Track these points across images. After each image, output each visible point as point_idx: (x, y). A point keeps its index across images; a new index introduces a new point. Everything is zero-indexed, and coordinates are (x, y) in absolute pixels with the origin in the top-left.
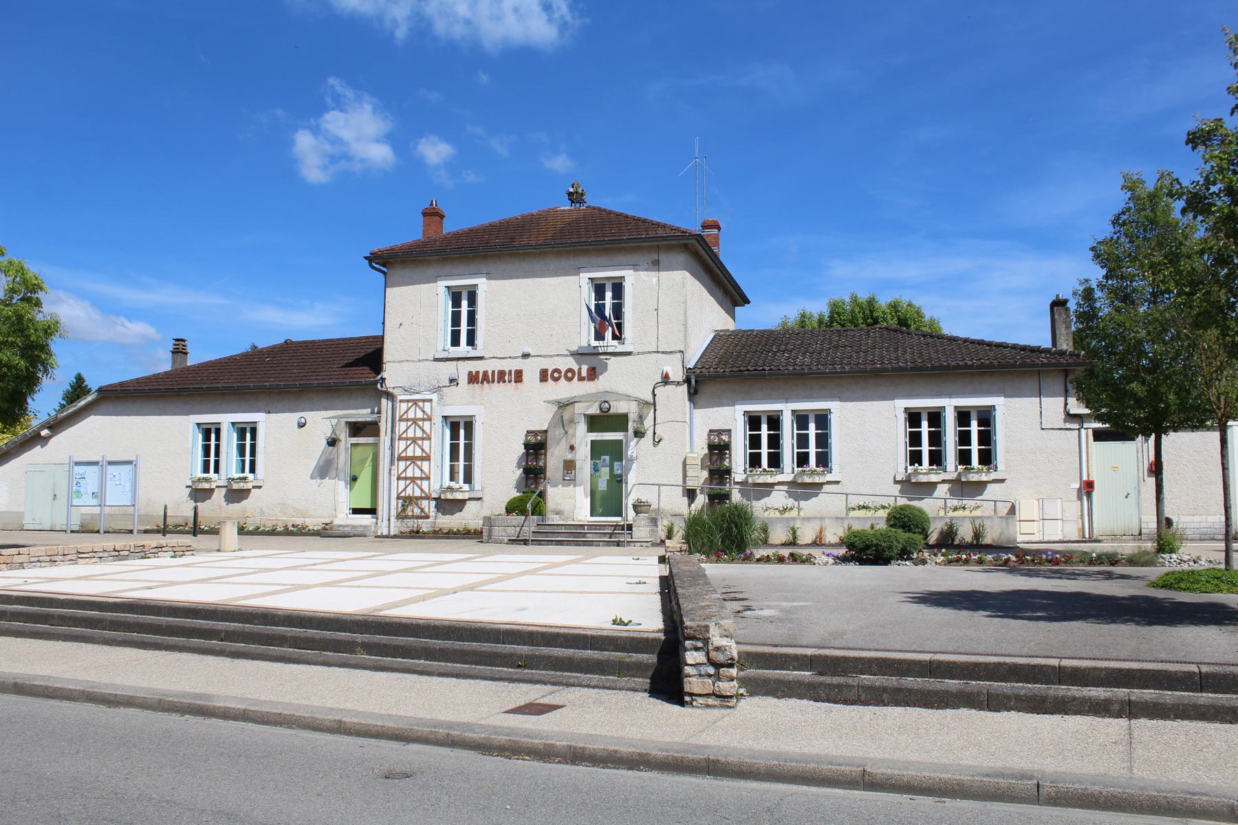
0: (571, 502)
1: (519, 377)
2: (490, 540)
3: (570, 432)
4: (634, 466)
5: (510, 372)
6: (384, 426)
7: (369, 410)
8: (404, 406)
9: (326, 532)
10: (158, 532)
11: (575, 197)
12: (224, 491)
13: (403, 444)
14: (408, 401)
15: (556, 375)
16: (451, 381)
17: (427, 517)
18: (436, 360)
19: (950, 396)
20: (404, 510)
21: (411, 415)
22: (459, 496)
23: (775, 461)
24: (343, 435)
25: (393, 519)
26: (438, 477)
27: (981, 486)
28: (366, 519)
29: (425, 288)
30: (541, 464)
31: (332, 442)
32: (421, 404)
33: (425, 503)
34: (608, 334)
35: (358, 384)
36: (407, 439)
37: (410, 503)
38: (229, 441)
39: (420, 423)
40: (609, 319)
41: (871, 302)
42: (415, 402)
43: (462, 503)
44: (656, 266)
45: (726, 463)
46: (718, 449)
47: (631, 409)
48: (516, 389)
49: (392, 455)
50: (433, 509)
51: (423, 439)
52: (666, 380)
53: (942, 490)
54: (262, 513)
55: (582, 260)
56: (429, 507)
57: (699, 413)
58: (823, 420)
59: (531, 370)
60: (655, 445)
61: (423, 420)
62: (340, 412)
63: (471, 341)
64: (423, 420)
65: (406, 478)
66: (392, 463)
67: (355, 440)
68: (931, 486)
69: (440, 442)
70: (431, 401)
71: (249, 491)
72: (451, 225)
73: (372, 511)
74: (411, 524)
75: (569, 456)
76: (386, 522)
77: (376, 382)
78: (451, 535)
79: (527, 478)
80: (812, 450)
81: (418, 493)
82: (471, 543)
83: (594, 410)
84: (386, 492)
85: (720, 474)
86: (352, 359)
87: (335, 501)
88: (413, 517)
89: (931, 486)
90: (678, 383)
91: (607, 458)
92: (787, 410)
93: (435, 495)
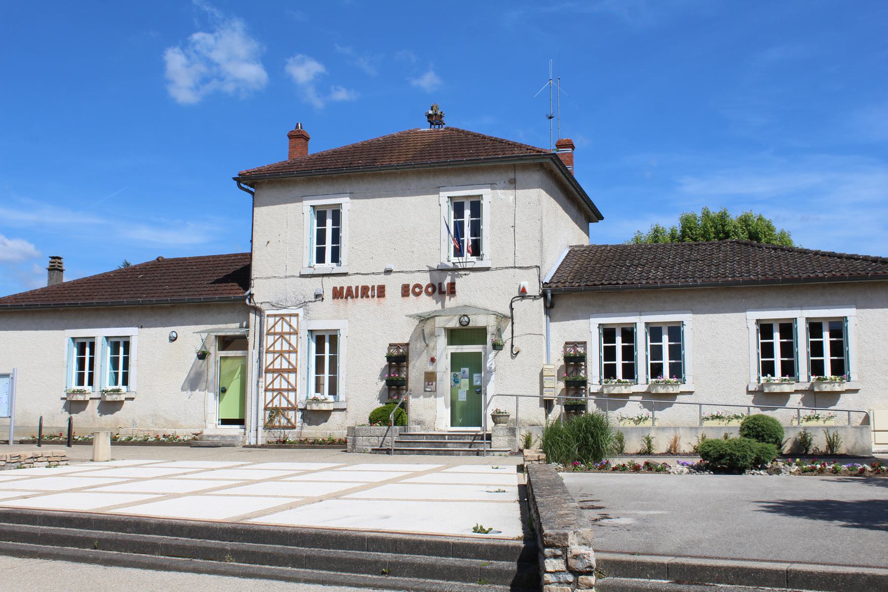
0: (432, 412)
1: (381, 292)
2: (354, 449)
3: (431, 345)
5: (373, 287)
6: (252, 340)
7: (238, 325)
8: (271, 321)
9: (196, 442)
10: (33, 442)
11: (435, 119)
12: (97, 402)
13: (270, 358)
14: (275, 316)
15: (417, 290)
16: (317, 296)
17: (294, 427)
18: (302, 276)
19: (801, 307)
20: (271, 421)
21: (278, 329)
22: (324, 407)
23: (630, 372)
25: (260, 429)
26: (304, 388)
27: (834, 396)
28: (235, 430)
30: (403, 376)
31: (202, 356)
32: (288, 319)
33: (291, 414)
35: (227, 299)
36: (274, 352)
37: (277, 414)
38: (103, 355)
39: (287, 337)
41: (723, 217)
42: (282, 317)
43: (328, 413)
44: (513, 184)
46: (574, 361)
49: (260, 367)
50: (299, 419)
51: (289, 352)
52: (523, 294)
53: (795, 400)
54: (134, 423)
55: (441, 180)
56: (296, 417)
57: (555, 326)
58: (676, 332)
59: (393, 285)
60: (512, 357)
61: (290, 334)
62: (210, 327)
63: (336, 258)
64: (290, 334)
65: (273, 390)
66: (260, 375)
67: (224, 353)
68: (785, 396)
69: (305, 355)
70: (297, 315)
71: (121, 402)
72: (315, 148)
73: (241, 422)
74: (278, 434)
75: (430, 368)
76: (253, 433)
77: (244, 298)
79: (390, 390)
80: (666, 361)
81: (284, 404)
83: (454, 324)
84: (254, 403)
85: (575, 385)
86: (222, 276)
87: (205, 412)
88: (280, 427)
89: (785, 396)
90: (535, 298)
91: (467, 370)
92: (640, 322)
93: (303, 407)
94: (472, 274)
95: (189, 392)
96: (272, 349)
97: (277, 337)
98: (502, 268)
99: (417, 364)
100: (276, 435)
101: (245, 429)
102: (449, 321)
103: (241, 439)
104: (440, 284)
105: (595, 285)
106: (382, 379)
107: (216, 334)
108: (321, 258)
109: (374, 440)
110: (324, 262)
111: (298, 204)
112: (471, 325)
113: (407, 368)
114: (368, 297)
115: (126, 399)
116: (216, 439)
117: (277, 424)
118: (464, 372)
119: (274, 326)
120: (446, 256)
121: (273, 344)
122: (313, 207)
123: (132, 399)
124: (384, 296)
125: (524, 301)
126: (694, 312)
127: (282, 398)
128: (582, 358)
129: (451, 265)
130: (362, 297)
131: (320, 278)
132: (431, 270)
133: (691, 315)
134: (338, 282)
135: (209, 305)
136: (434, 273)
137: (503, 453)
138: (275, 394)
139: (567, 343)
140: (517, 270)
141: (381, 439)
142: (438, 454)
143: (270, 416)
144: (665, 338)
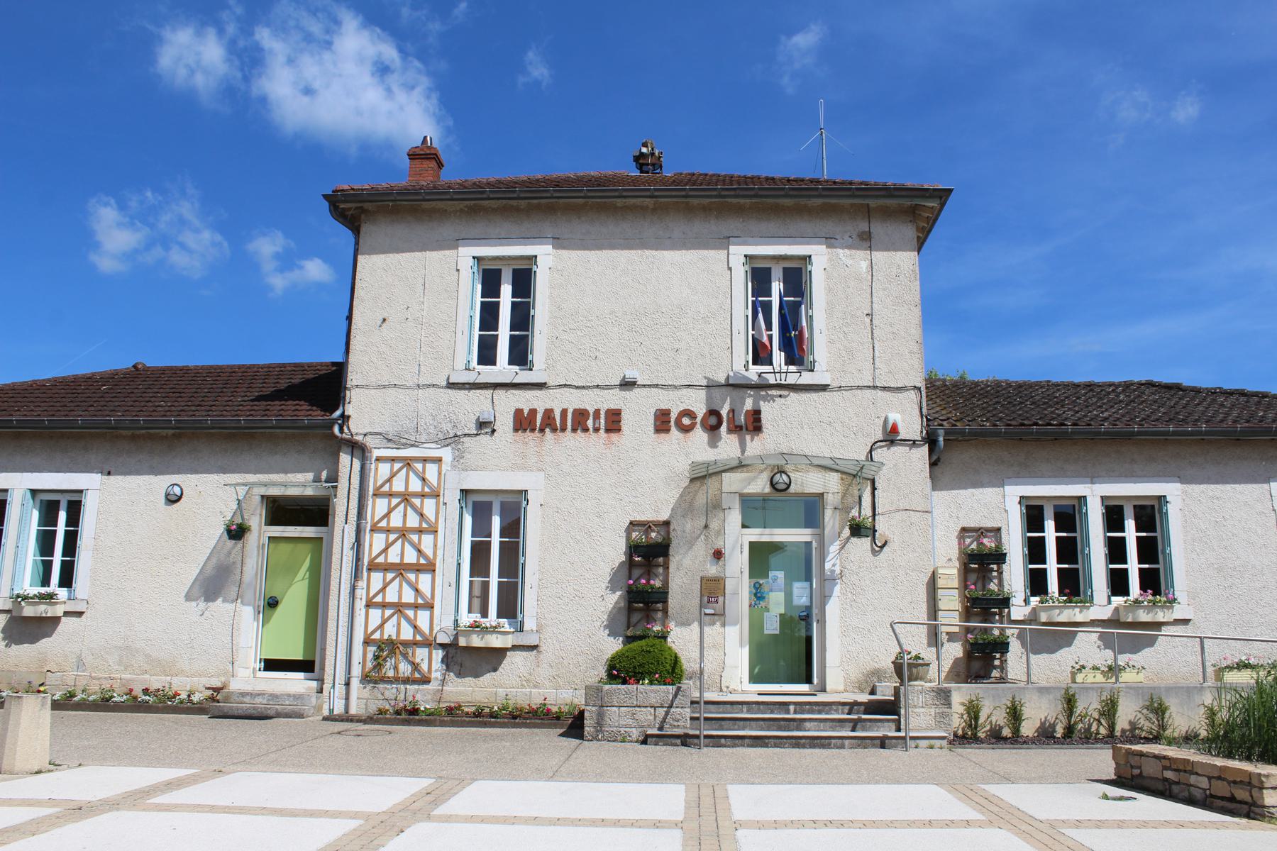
0: (721, 657)
1: (614, 421)
3: (714, 525)
4: (837, 589)
5: (597, 412)
6: (343, 508)
7: (310, 476)
8: (384, 469)
9: (216, 706)
13: (379, 541)
14: (393, 460)
15: (686, 421)
16: (482, 425)
17: (426, 681)
18: (452, 386)
21: (398, 486)
22: (495, 641)
23: (1072, 585)
24: (256, 519)
25: (355, 683)
26: (449, 606)
28: (295, 682)
29: (435, 259)
30: (657, 583)
31: (237, 532)
32: (419, 466)
33: (421, 654)
34: (778, 357)
36: (388, 531)
37: (392, 653)
39: (417, 501)
40: (785, 326)
42: (408, 462)
44: (866, 240)
45: (993, 586)
46: (981, 560)
47: (830, 485)
48: (609, 444)
49: (358, 559)
50: (437, 663)
51: (420, 531)
52: (891, 436)
54: (80, 663)
55: (732, 225)
58: (1150, 515)
59: (638, 411)
60: (874, 553)
61: (423, 496)
62: (251, 478)
63: (520, 354)
64: (423, 496)
65: (384, 605)
66: (357, 575)
67: (277, 531)
69: (451, 540)
70: (438, 460)
71: (55, 621)
73: (305, 666)
74: (393, 695)
75: (712, 570)
76: (340, 690)
78: (483, 717)
79: (630, 610)
81: (407, 634)
82: (550, 740)
83: (760, 485)
85: (985, 606)
90: (914, 443)
91: (780, 575)
92: (1094, 495)
93: (443, 639)
94: (794, 396)
95: (202, 604)
96: (383, 524)
97: (395, 501)
98: (851, 388)
99: (687, 562)
100: (387, 694)
101: (321, 680)
103: (314, 700)
105: (1022, 425)
106: (613, 590)
107: (263, 491)
109: (646, 716)
110: (494, 363)
111: (447, 252)
112: (792, 489)
113: (666, 568)
114: (586, 430)
115: (66, 614)
116: (258, 700)
117: (391, 673)
118: (775, 579)
119: (389, 480)
120: (740, 363)
121: (387, 515)
122: (478, 259)
123: (80, 614)
124: (619, 430)
125: (893, 449)
126: (1184, 480)
127: (403, 622)
128: (999, 557)
129: (755, 378)
132: (711, 386)
133: (1179, 485)
134: (525, 400)
135: (252, 436)
136: (716, 393)
137: (937, 743)
138: (388, 612)
139: (964, 530)
140: (880, 393)
141: (661, 712)
142: (797, 746)
143: (376, 657)
144: (1130, 524)
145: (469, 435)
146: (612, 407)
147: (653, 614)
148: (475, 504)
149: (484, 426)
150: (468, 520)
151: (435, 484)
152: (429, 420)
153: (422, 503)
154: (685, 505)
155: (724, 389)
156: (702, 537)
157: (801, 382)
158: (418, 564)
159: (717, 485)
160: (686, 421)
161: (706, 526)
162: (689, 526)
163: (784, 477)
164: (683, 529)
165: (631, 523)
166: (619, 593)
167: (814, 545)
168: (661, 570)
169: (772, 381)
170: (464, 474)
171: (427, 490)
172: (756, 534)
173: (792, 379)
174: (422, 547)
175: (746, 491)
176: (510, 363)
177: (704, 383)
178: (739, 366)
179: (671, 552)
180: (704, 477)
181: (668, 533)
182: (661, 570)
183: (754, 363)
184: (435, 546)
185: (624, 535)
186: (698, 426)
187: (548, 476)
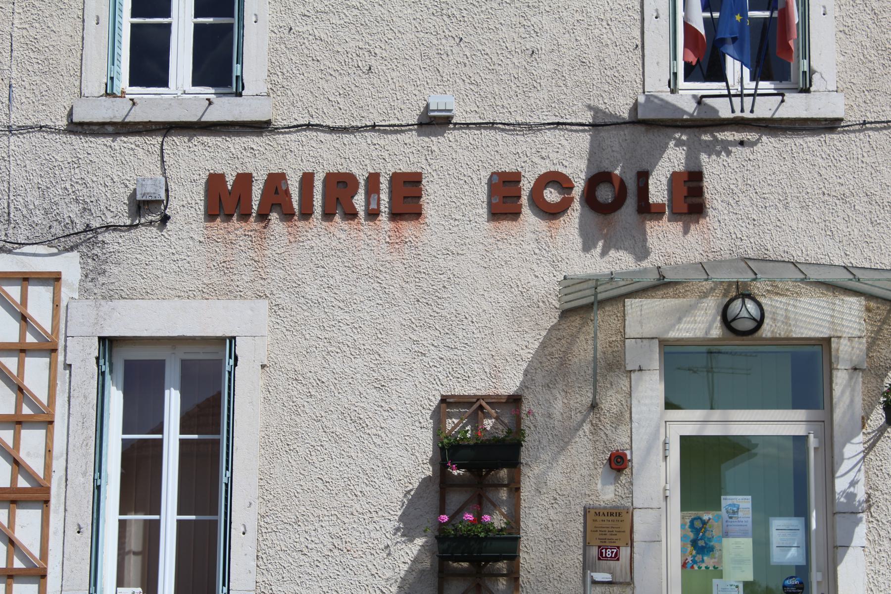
1: (407, 197)
3: (610, 402)
5: (373, 180)
15: (552, 195)
18: (77, 128)
30: (497, 520)
59: (455, 176)
63: (216, 62)
69: (80, 440)
70: (53, 279)
75: (607, 494)
83: (700, 323)
91: (744, 503)
94: (769, 143)
99: (555, 477)
102: (681, 315)
104: (643, 177)
108: (149, 65)
110: (164, 83)
112: (767, 330)
113: (515, 489)
114: (351, 215)
118: (734, 512)
120: (659, 75)
124: (416, 214)
129: (689, 107)
130: (328, 215)
131: (155, 141)
132: (601, 124)
136: (614, 139)
145: (115, 228)
146: (404, 168)
147: (488, 583)
148: (129, 366)
149: (147, 209)
150: (116, 398)
151: (47, 326)
152: (33, 196)
153: (21, 366)
154: (551, 363)
155: (627, 131)
156: (587, 427)
157: (785, 112)
158: (14, 489)
159: (615, 323)
160: (552, 195)
161: (594, 406)
162: (558, 406)
163: (750, 305)
164: (547, 410)
165: (444, 400)
166: (420, 541)
167: (813, 442)
168: (504, 494)
169: (725, 112)
170: (106, 306)
171: (30, 339)
172: (693, 422)
173: (765, 109)
174: (23, 455)
175: (673, 334)
176: (195, 83)
177: (588, 117)
178: (657, 84)
179: (524, 457)
180: (589, 307)
181: (518, 419)
182: (504, 494)
183: (687, 79)
184: (49, 451)
185: (430, 424)
186: (576, 205)
187: (276, 309)
